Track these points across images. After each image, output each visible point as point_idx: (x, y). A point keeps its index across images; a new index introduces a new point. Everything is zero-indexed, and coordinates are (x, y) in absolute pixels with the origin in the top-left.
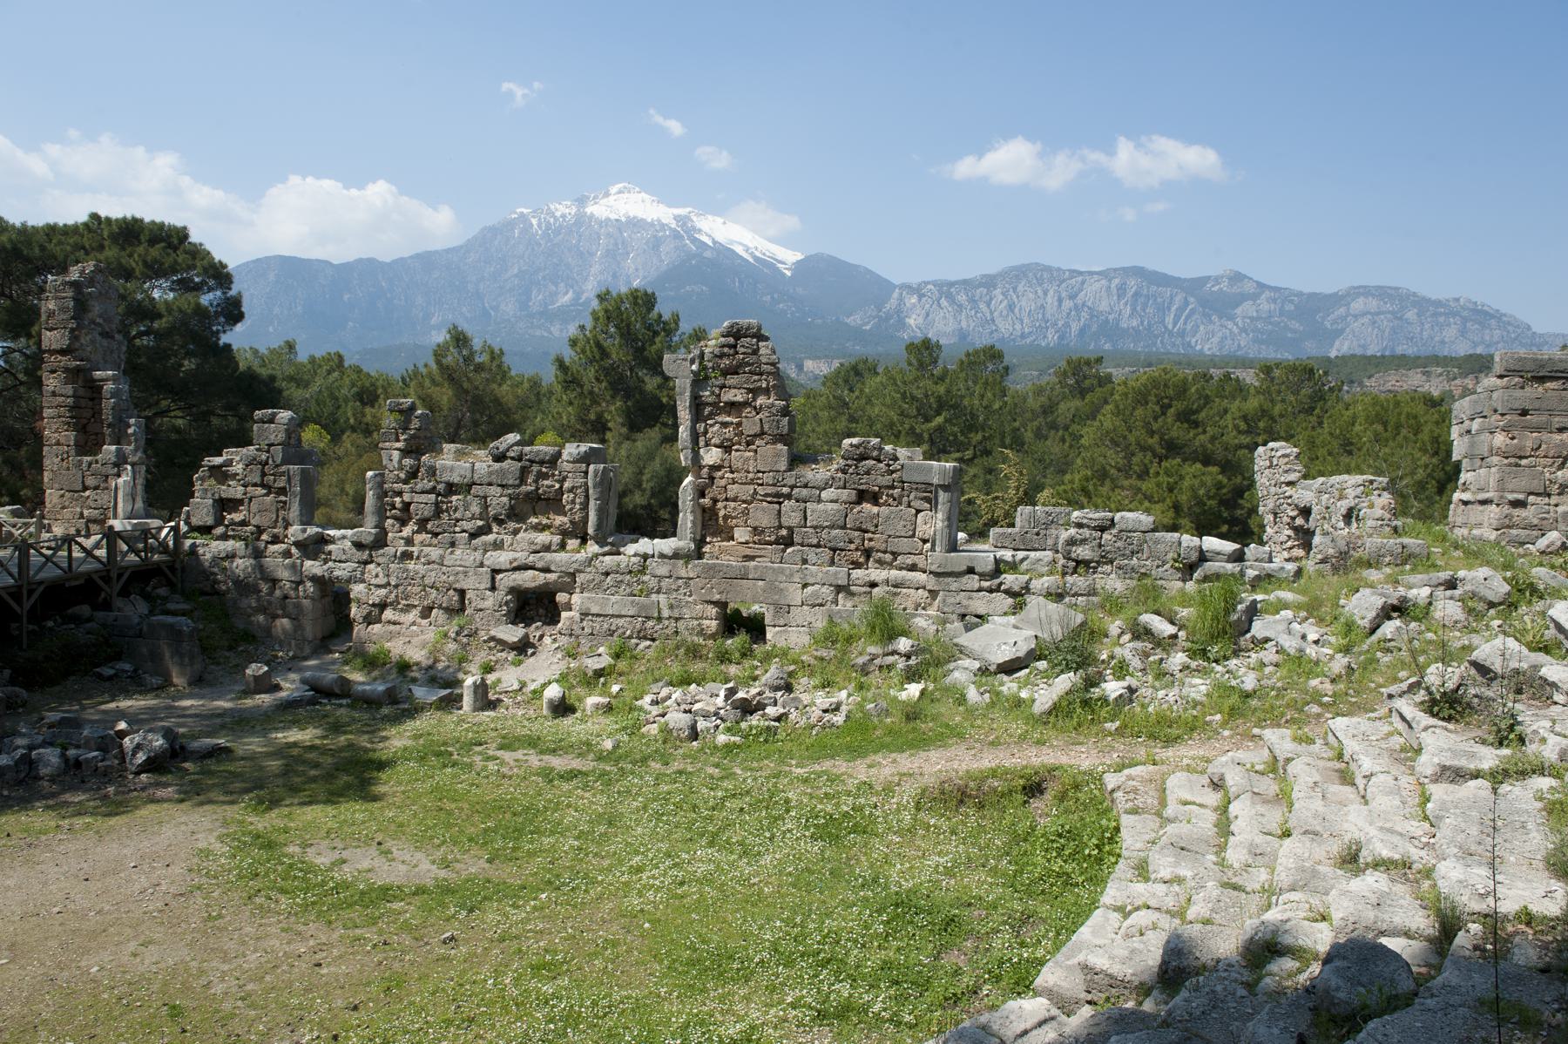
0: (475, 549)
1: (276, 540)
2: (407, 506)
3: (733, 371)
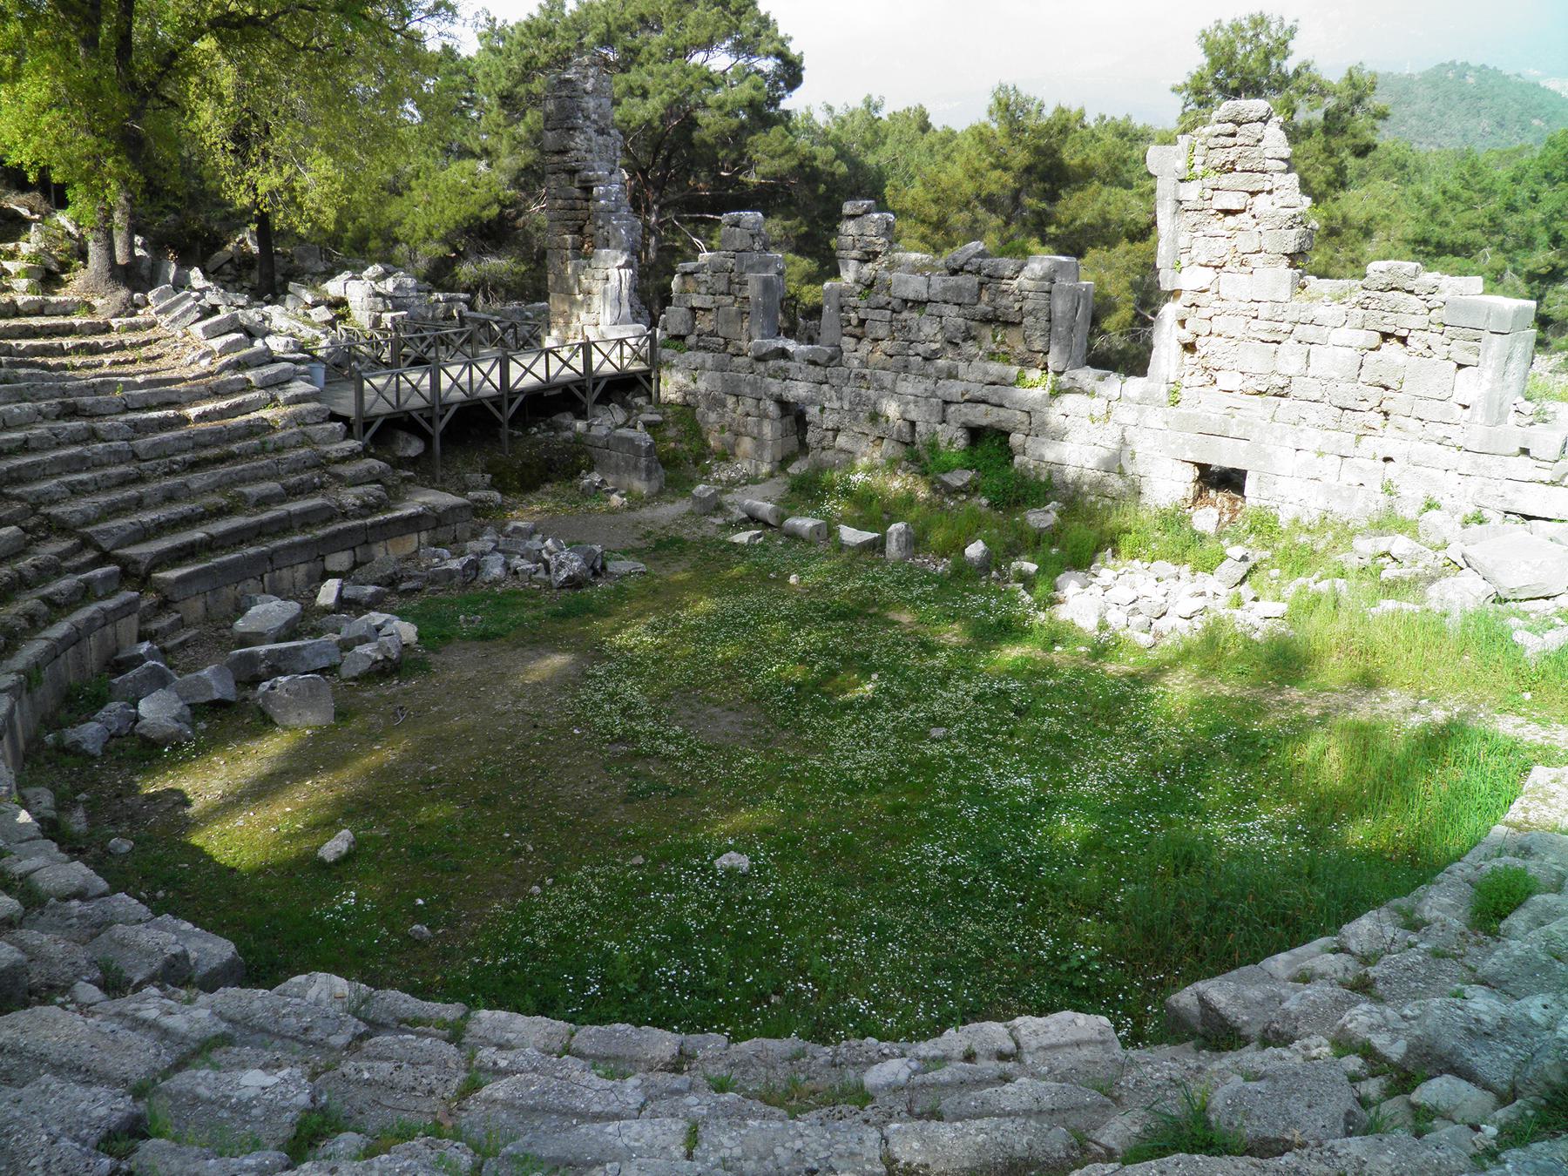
0: (928, 377)
2: (862, 322)
3: (1228, 168)
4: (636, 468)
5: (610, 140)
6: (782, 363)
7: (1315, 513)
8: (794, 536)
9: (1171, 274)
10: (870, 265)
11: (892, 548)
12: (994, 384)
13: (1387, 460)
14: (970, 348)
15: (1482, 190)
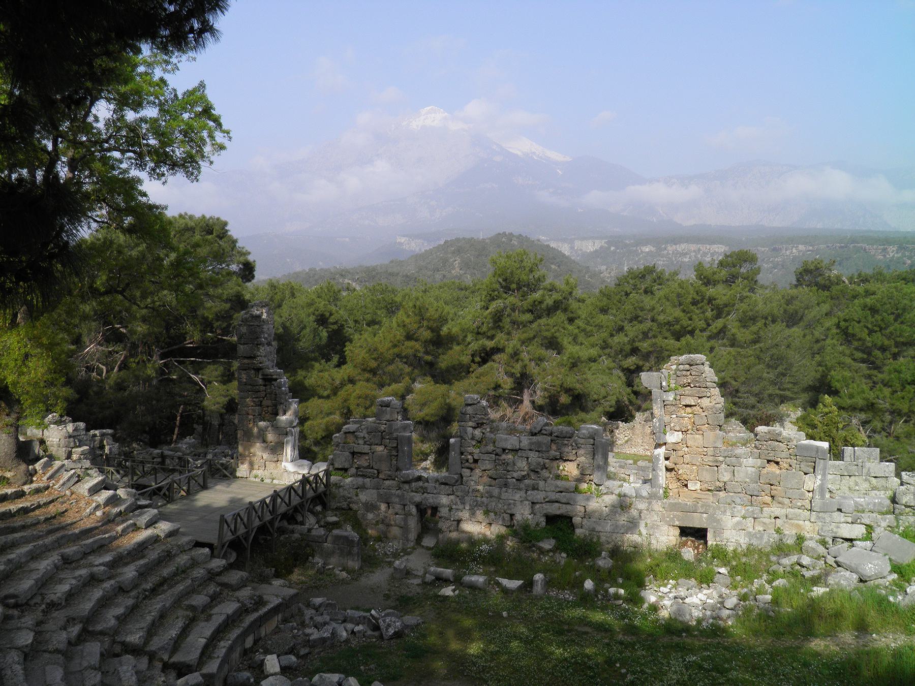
0: (520, 489)
1: (390, 478)
2: (476, 461)
4: (350, 553)
5: (272, 349)
6: (421, 483)
7: (744, 546)
8: (472, 587)
9: (662, 435)
10: (479, 430)
11: (538, 589)
12: (561, 492)
13: (775, 518)
14: (545, 473)
15: (595, 326)
